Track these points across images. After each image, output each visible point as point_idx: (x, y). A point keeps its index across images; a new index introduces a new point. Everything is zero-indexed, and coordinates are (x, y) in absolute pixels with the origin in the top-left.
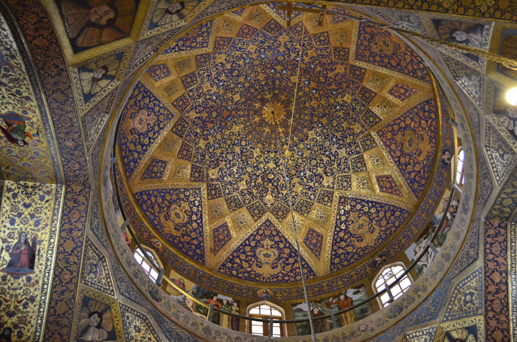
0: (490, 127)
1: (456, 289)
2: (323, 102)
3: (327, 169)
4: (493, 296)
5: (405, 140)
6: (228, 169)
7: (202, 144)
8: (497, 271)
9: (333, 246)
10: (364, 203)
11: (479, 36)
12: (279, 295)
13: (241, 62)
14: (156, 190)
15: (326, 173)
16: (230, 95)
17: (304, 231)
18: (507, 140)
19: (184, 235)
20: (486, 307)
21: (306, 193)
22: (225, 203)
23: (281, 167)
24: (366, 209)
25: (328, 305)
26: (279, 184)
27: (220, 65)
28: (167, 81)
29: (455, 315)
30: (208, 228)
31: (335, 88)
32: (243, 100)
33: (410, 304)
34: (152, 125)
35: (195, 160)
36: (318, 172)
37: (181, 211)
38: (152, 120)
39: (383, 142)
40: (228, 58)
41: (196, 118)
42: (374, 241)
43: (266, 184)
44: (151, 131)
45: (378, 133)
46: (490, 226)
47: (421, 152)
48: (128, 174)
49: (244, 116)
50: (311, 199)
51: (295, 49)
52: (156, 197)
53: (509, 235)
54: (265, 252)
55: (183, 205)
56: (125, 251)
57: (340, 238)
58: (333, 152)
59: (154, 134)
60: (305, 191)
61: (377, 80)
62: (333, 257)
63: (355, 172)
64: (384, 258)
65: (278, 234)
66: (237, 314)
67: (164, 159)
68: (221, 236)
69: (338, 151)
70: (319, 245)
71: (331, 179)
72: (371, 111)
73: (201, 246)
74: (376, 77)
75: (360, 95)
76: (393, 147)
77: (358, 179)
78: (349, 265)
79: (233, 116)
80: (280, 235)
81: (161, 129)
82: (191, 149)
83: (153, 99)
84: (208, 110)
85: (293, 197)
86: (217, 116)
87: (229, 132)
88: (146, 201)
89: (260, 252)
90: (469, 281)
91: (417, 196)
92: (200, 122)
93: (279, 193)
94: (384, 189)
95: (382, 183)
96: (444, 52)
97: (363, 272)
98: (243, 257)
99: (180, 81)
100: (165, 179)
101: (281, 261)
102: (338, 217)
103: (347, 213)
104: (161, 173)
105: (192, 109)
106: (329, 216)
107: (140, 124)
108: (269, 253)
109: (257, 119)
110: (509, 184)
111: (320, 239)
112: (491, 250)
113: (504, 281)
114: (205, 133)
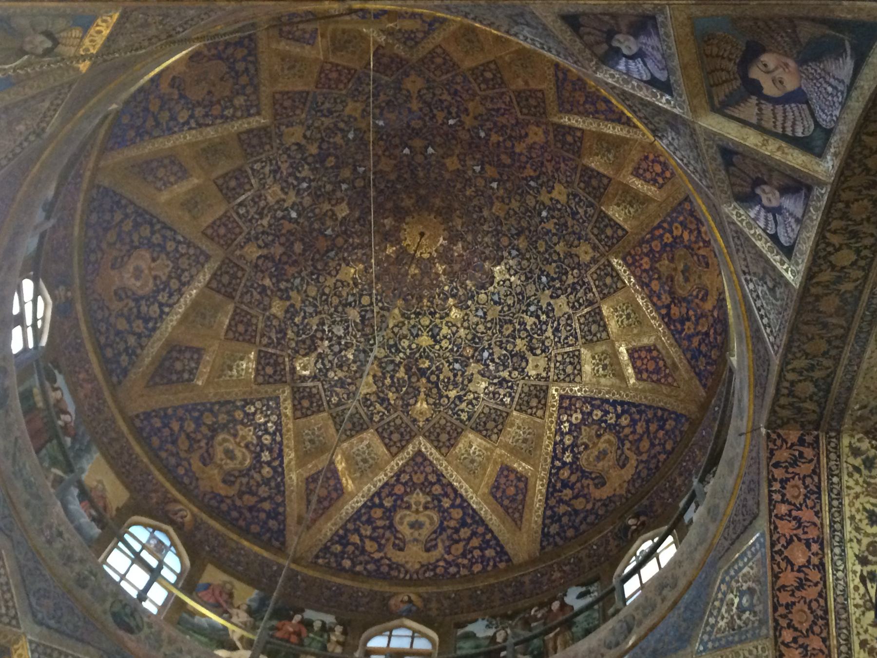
0: (739, 233)
1: (723, 581)
2: (515, 205)
3: (534, 341)
4: (793, 595)
5: (675, 269)
6: (335, 354)
7: (277, 308)
8: (799, 540)
9: (547, 499)
10: (607, 407)
11: (653, 41)
12: (434, 605)
13: (338, 139)
14: (182, 406)
15: (532, 349)
16: (326, 207)
17: (491, 471)
18: (769, 256)
19: (244, 493)
20: (775, 621)
21: (494, 393)
22: (330, 422)
23: (445, 344)
24: (611, 419)
25: (527, 623)
26: (441, 377)
27: (294, 148)
28: (184, 189)
29: (720, 640)
30: (294, 477)
31: (532, 174)
32: (357, 214)
33: (645, 616)
34: (164, 278)
35: (265, 341)
36: (517, 349)
37: (238, 444)
38: (164, 268)
39: (635, 277)
40: (308, 133)
41: (259, 258)
42: (625, 485)
43: (414, 380)
44: (164, 290)
45: (624, 259)
46: (779, 442)
47: (706, 294)
48: (115, 379)
49: (362, 246)
50: (503, 404)
51: (441, 101)
52: (181, 420)
53: (824, 460)
54: (412, 518)
55: (241, 433)
56: (60, 534)
57: (563, 481)
58: (544, 306)
59: (171, 295)
60: (491, 389)
61: (609, 151)
62: (547, 521)
63: (588, 343)
64: (642, 518)
65: (439, 481)
66: (339, 650)
67: (196, 344)
68: (325, 490)
69: (552, 302)
70: (520, 497)
71: (542, 362)
72: (606, 216)
73: (279, 514)
74: (605, 145)
75: (582, 185)
76: (655, 286)
77: (594, 358)
78: (576, 536)
79: (340, 248)
80: (444, 481)
81: (184, 284)
82: (254, 321)
83: (158, 227)
84: (283, 240)
85: (470, 403)
86: (304, 250)
87: (334, 280)
88: (159, 430)
89: (401, 518)
90: (745, 564)
91: (704, 386)
92: (270, 264)
93: (441, 396)
94: (645, 376)
95: (639, 363)
96: (610, 81)
97: (602, 549)
98: (367, 531)
99: (214, 187)
100: (200, 383)
101: (444, 536)
102: (558, 438)
103: (575, 428)
104: (191, 372)
105: (248, 240)
106: (540, 437)
107: (137, 278)
108: (422, 519)
109: (390, 250)
110: (794, 349)
111: (522, 485)
112: (783, 495)
113: (815, 560)
114: (283, 285)
